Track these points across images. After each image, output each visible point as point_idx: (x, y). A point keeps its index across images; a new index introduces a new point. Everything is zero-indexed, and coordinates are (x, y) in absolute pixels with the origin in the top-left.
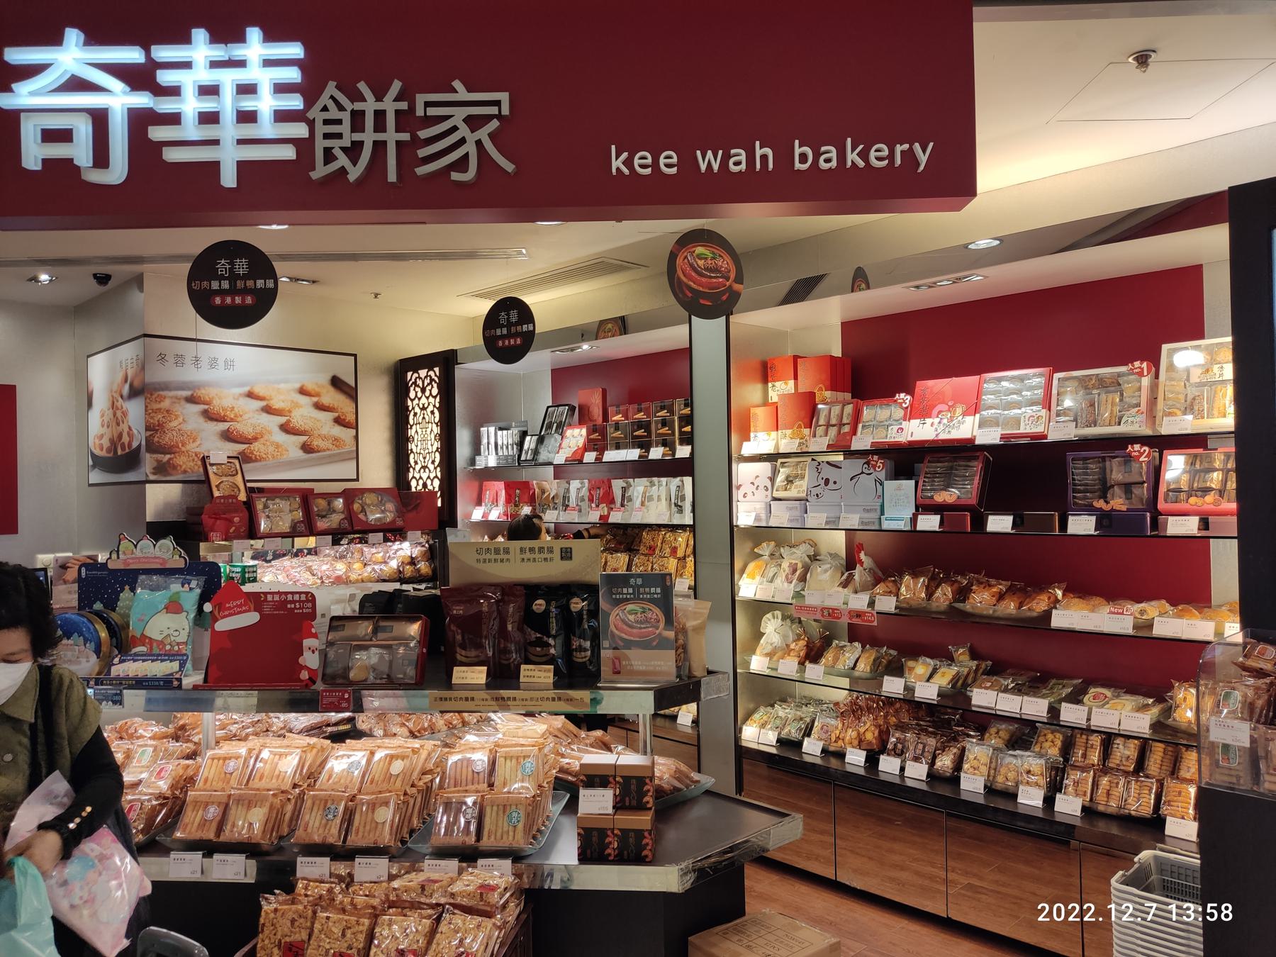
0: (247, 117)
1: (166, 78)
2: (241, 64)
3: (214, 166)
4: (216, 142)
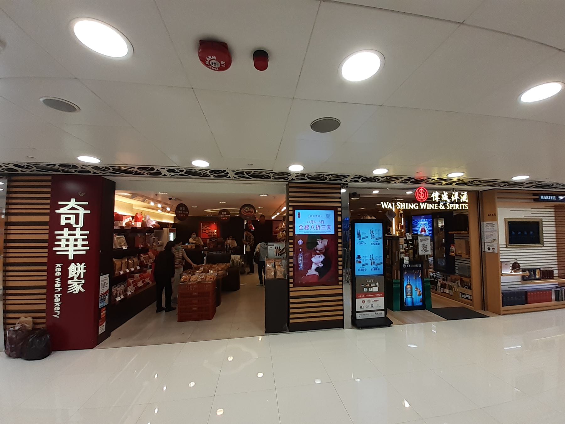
0: (75, 246)
1: (58, 237)
2: (74, 235)
3: (68, 255)
4: (68, 251)
